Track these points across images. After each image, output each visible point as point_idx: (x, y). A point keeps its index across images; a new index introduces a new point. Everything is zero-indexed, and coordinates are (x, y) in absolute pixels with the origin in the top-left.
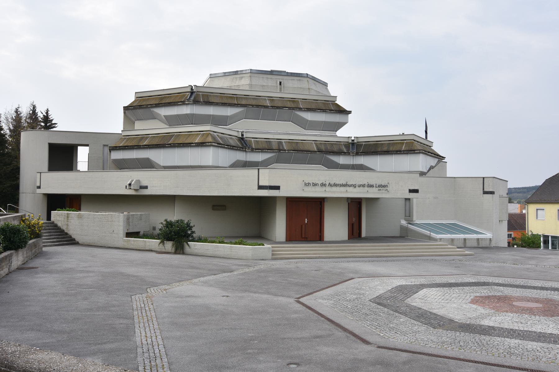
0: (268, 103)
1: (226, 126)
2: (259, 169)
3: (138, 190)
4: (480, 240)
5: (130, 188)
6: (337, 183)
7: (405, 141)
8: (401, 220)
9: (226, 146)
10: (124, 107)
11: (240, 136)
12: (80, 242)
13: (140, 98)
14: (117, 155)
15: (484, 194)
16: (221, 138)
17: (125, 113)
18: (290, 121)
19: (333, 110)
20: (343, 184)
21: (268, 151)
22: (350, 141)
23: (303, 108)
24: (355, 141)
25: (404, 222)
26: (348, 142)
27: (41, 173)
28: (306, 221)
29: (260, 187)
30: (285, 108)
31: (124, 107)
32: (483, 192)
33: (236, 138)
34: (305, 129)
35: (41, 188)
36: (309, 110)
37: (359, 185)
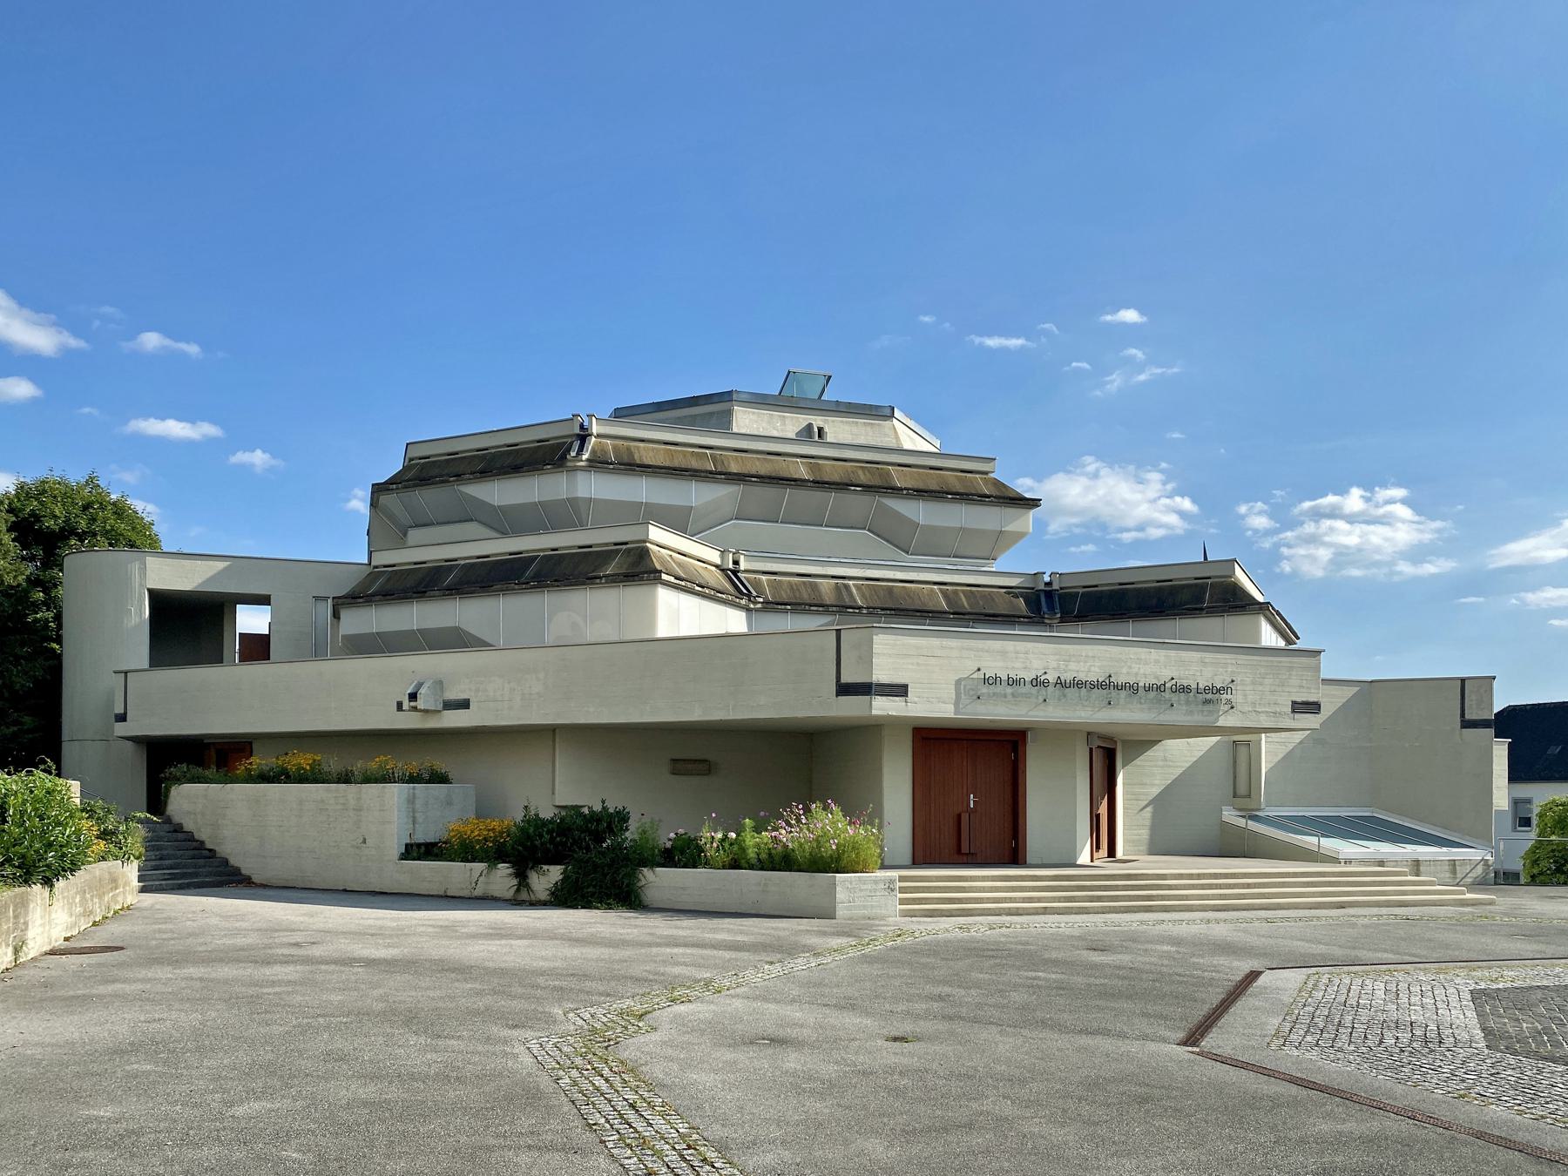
0: (803, 472)
2: (838, 631)
3: (440, 711)
4: (1457, 863)
5: (415, 709)
6: (1082, 677)
7: (1209, 581)
8: (1223, 807)
9: (698, 585)
10: (373, 485)
11: (731, 566)
12: (255, 879)
13: (423, 461)
14: (358, 621)
16: (679, 565)
17: (374, 504)
18: (864, 529)
19: (988, 497)
20: (1098, 681)
21: (812, 608)
22: (1042, 587)
23: (905, 489)
24: (1056, 586)
25: (1230, 816)
26: (1033, 589)
27: (126, 673)
28: (972, 802)
29: (844, 689)
30: (853, 488)
31: (373, 485)
34: (907, 553)
35: (128, 719)
36: (921, 493)
37: (1147, 685)
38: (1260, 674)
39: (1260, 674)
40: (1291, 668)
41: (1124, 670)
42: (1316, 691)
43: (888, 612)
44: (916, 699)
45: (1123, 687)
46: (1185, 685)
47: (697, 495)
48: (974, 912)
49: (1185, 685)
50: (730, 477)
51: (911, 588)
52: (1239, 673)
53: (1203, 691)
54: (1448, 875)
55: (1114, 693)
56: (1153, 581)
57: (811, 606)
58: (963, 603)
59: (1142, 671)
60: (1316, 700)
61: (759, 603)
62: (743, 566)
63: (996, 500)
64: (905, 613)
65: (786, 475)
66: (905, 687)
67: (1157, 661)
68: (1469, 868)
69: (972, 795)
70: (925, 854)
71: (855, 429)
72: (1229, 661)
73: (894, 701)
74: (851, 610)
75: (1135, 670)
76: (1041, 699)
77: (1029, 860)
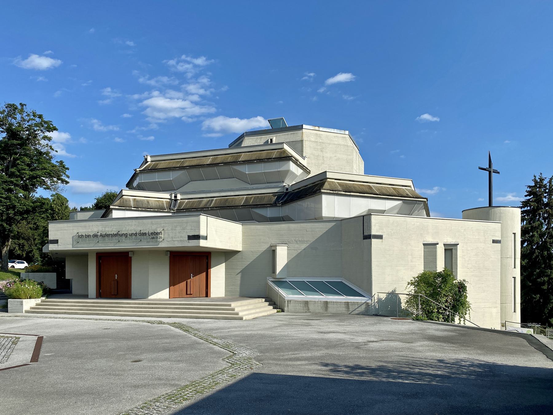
1: (175, 190)
4: (349, 304)
9: (133, 208)
15: (364, 239)
20: (114, 234)
21: (192, 210)
24: (289, 190)
28: (116, 277)
30: (220, 165)
32: (363, 236)
33: (168, 200)
38: (174, 226)
39: (174, 226)
40: (187, 223)
41: (124, 229)
42: (198, 231)
43: (219, 208)
44: (61, 244)
45: (122, 235)
46: (144, 233)
47: (171, 176)
48: (99, 314)
49: (144, 233)
50: (180, 168)
51: (236, 198)
52: (166, 226)
53: (150, 234)
54: (344, 309)
55: (120, 238)
56: (311, 184)
57: (192, 209)
58: (250, 202)
59: (130, 229)
60: (198, 234)
61: (175, 210)
62: (179, 197)
63: (274, 160)
64: (224, 208)
65: (201, 164)
66: (58, 240)
67: (135, 225)
68: (357, 306)
69: (116, 275)
70: (100, 295)
71: (286, 137)
72: (162, 222)
73: (55, 245)
74: (205, 209)
75: (127, 229)
76: (97, 242)
77: (132, 297)
